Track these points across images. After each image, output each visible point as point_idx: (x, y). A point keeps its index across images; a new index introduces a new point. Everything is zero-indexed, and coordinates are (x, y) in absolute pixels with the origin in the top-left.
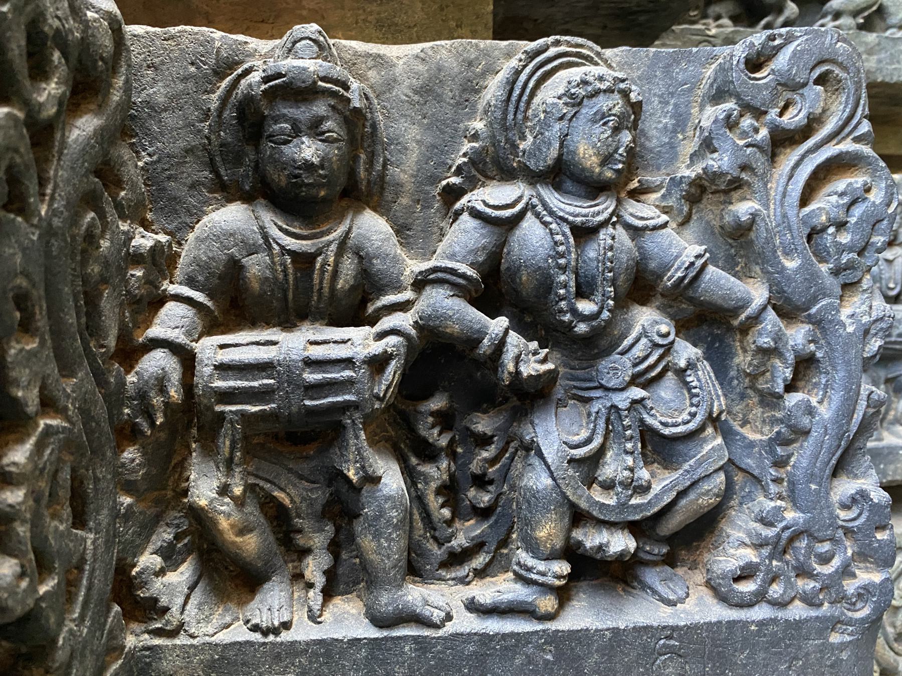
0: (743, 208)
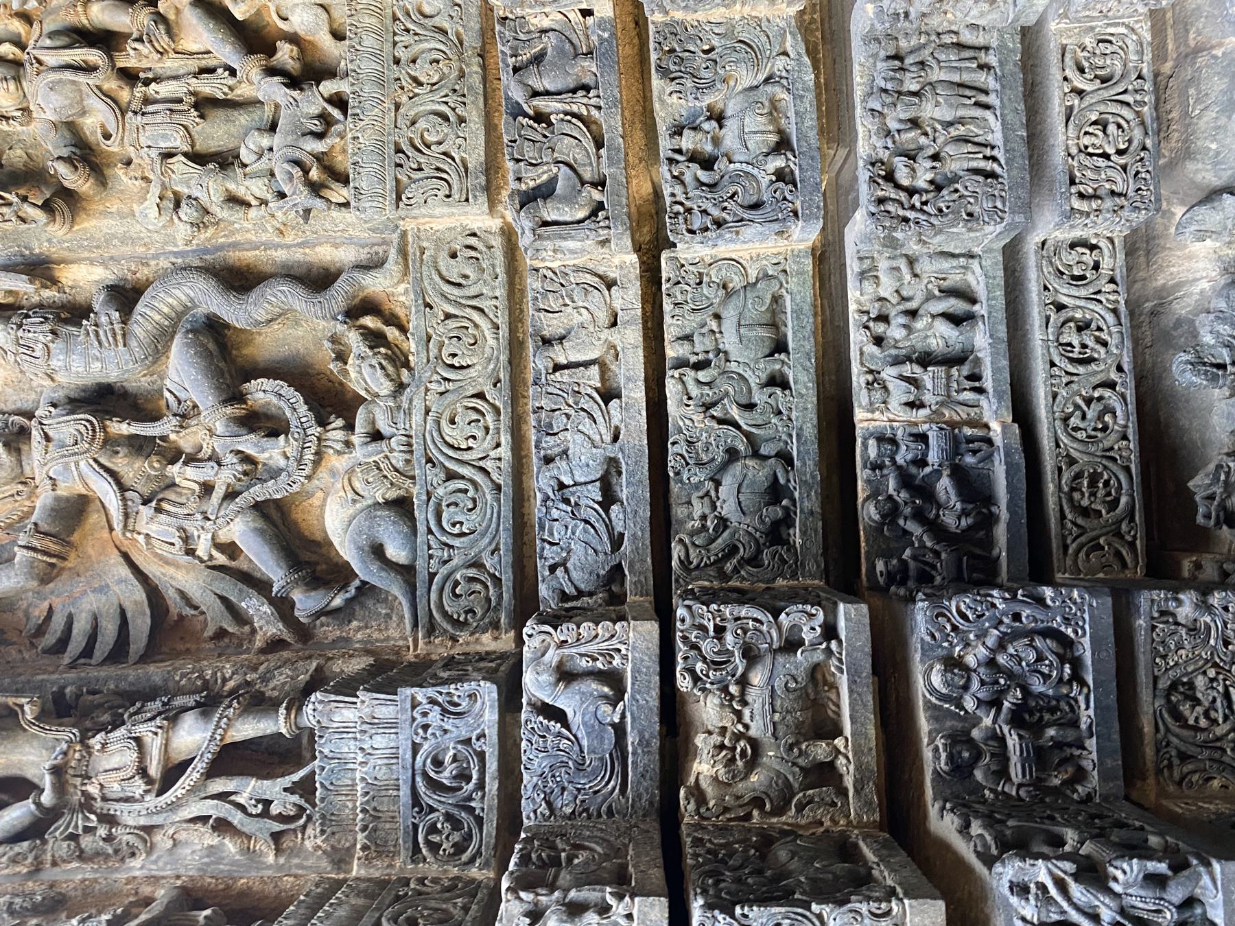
0: (972, 636)
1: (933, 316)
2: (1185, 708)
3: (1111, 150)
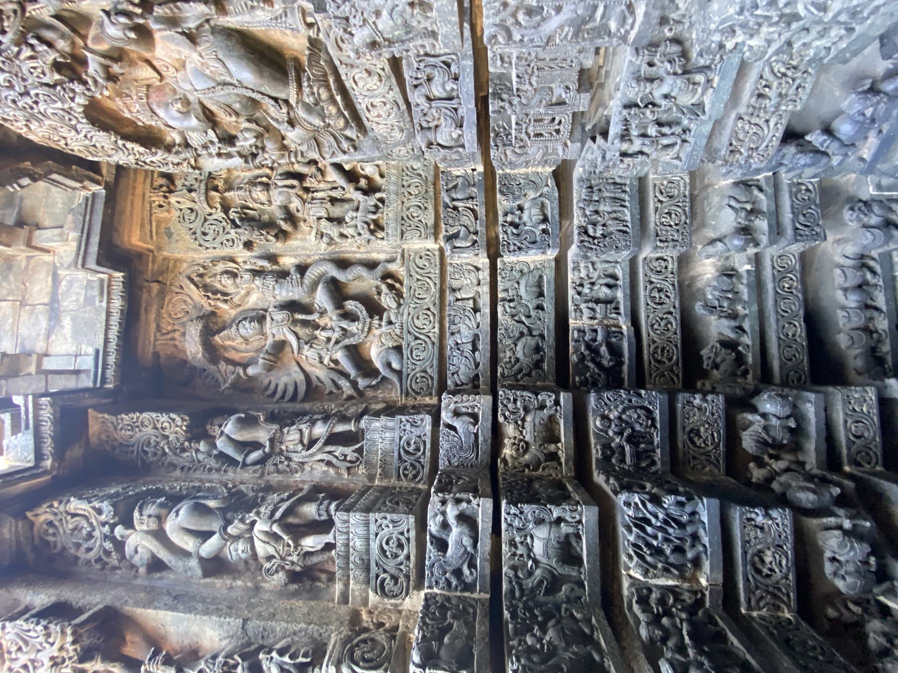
2: (696, 439)
3: (672, 224)
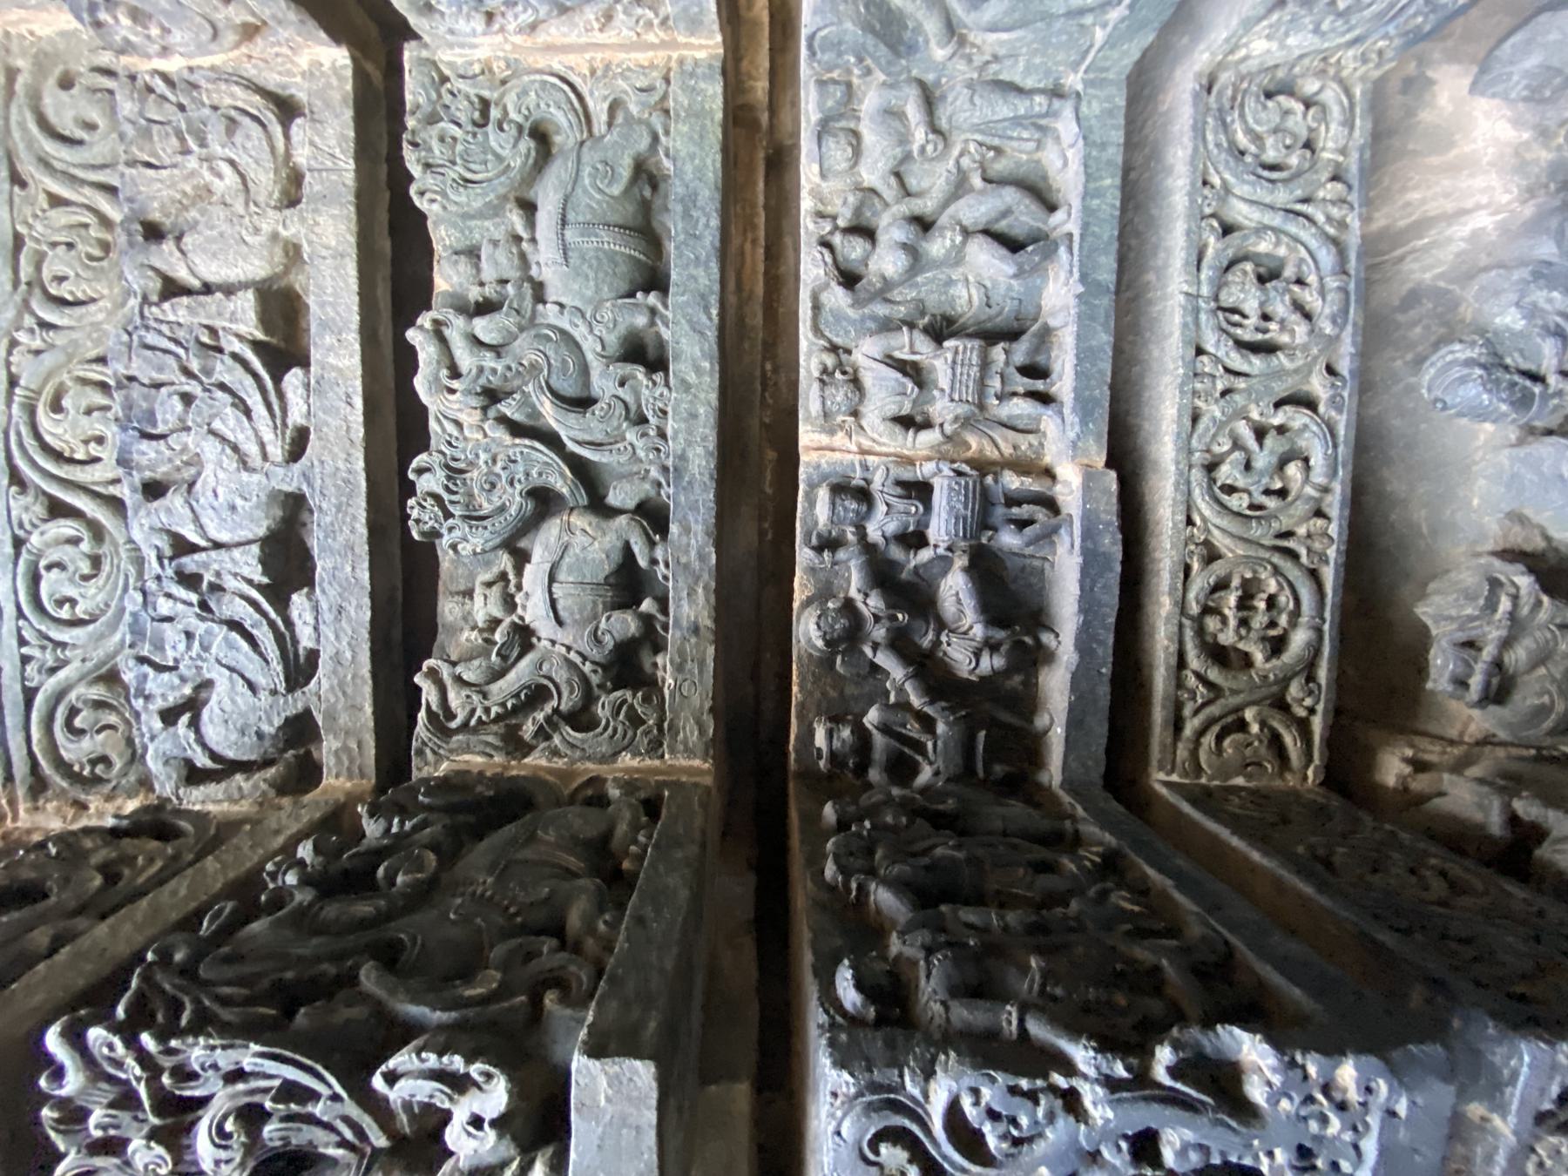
1: (966, 233)
